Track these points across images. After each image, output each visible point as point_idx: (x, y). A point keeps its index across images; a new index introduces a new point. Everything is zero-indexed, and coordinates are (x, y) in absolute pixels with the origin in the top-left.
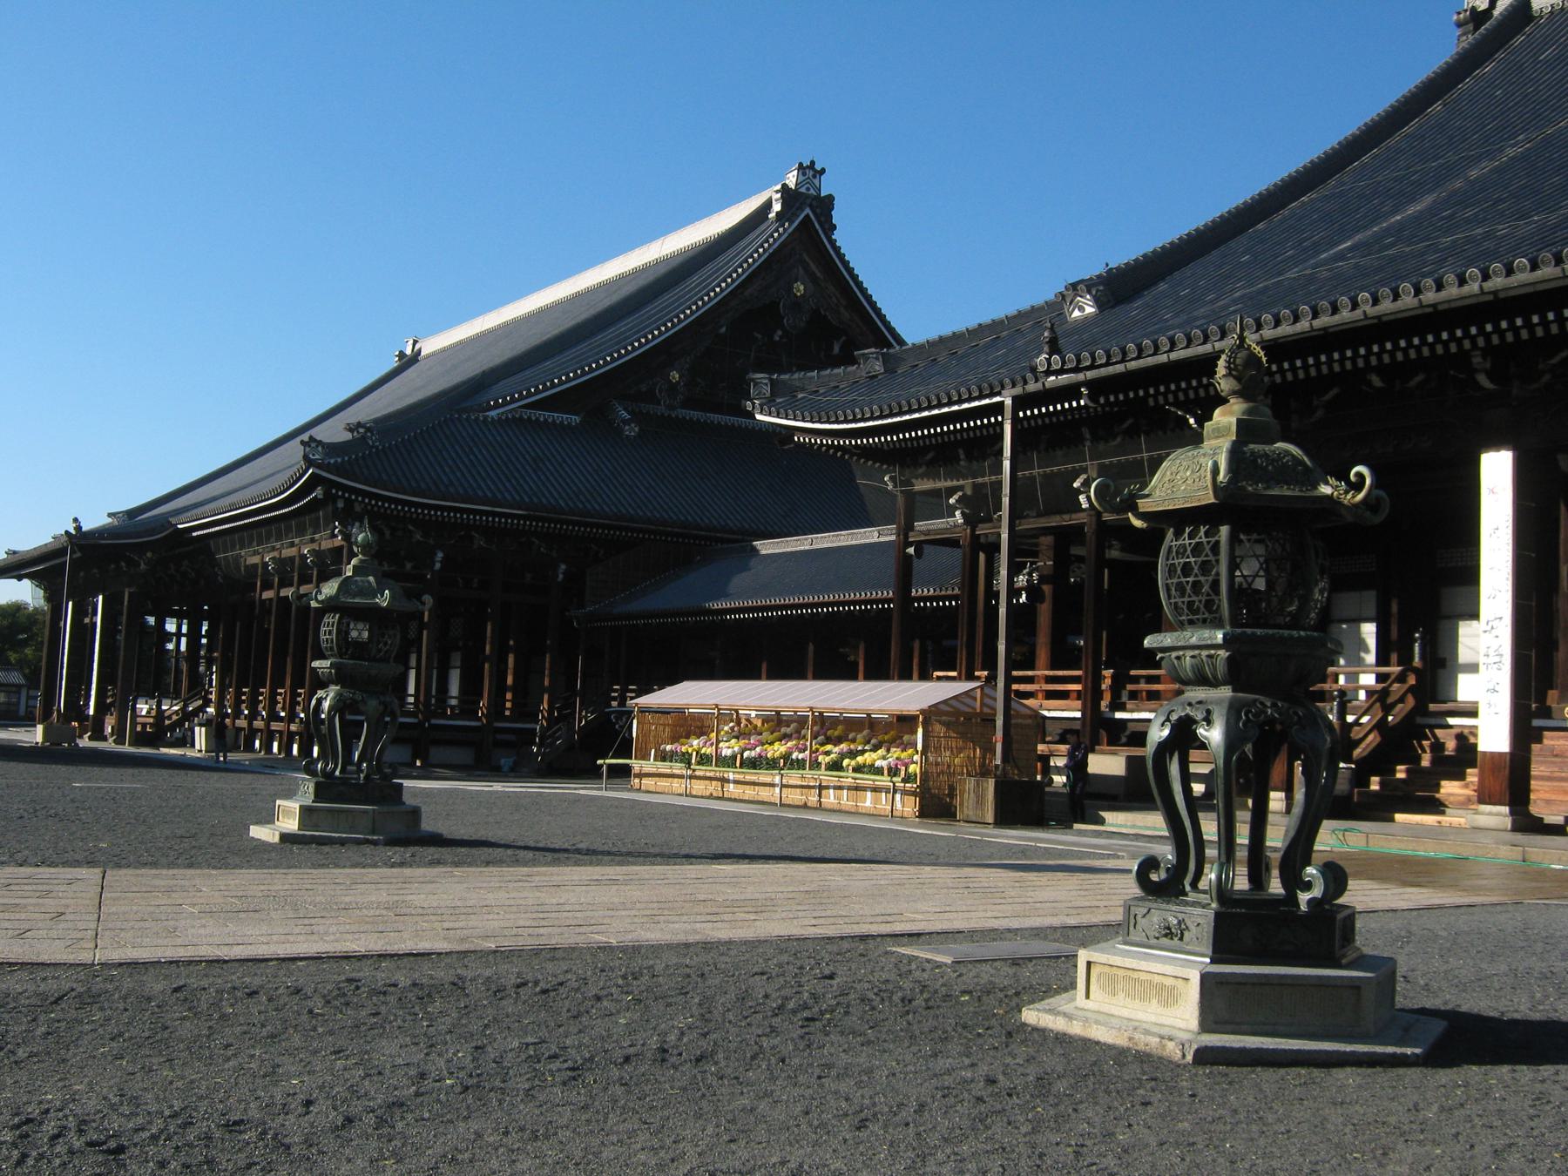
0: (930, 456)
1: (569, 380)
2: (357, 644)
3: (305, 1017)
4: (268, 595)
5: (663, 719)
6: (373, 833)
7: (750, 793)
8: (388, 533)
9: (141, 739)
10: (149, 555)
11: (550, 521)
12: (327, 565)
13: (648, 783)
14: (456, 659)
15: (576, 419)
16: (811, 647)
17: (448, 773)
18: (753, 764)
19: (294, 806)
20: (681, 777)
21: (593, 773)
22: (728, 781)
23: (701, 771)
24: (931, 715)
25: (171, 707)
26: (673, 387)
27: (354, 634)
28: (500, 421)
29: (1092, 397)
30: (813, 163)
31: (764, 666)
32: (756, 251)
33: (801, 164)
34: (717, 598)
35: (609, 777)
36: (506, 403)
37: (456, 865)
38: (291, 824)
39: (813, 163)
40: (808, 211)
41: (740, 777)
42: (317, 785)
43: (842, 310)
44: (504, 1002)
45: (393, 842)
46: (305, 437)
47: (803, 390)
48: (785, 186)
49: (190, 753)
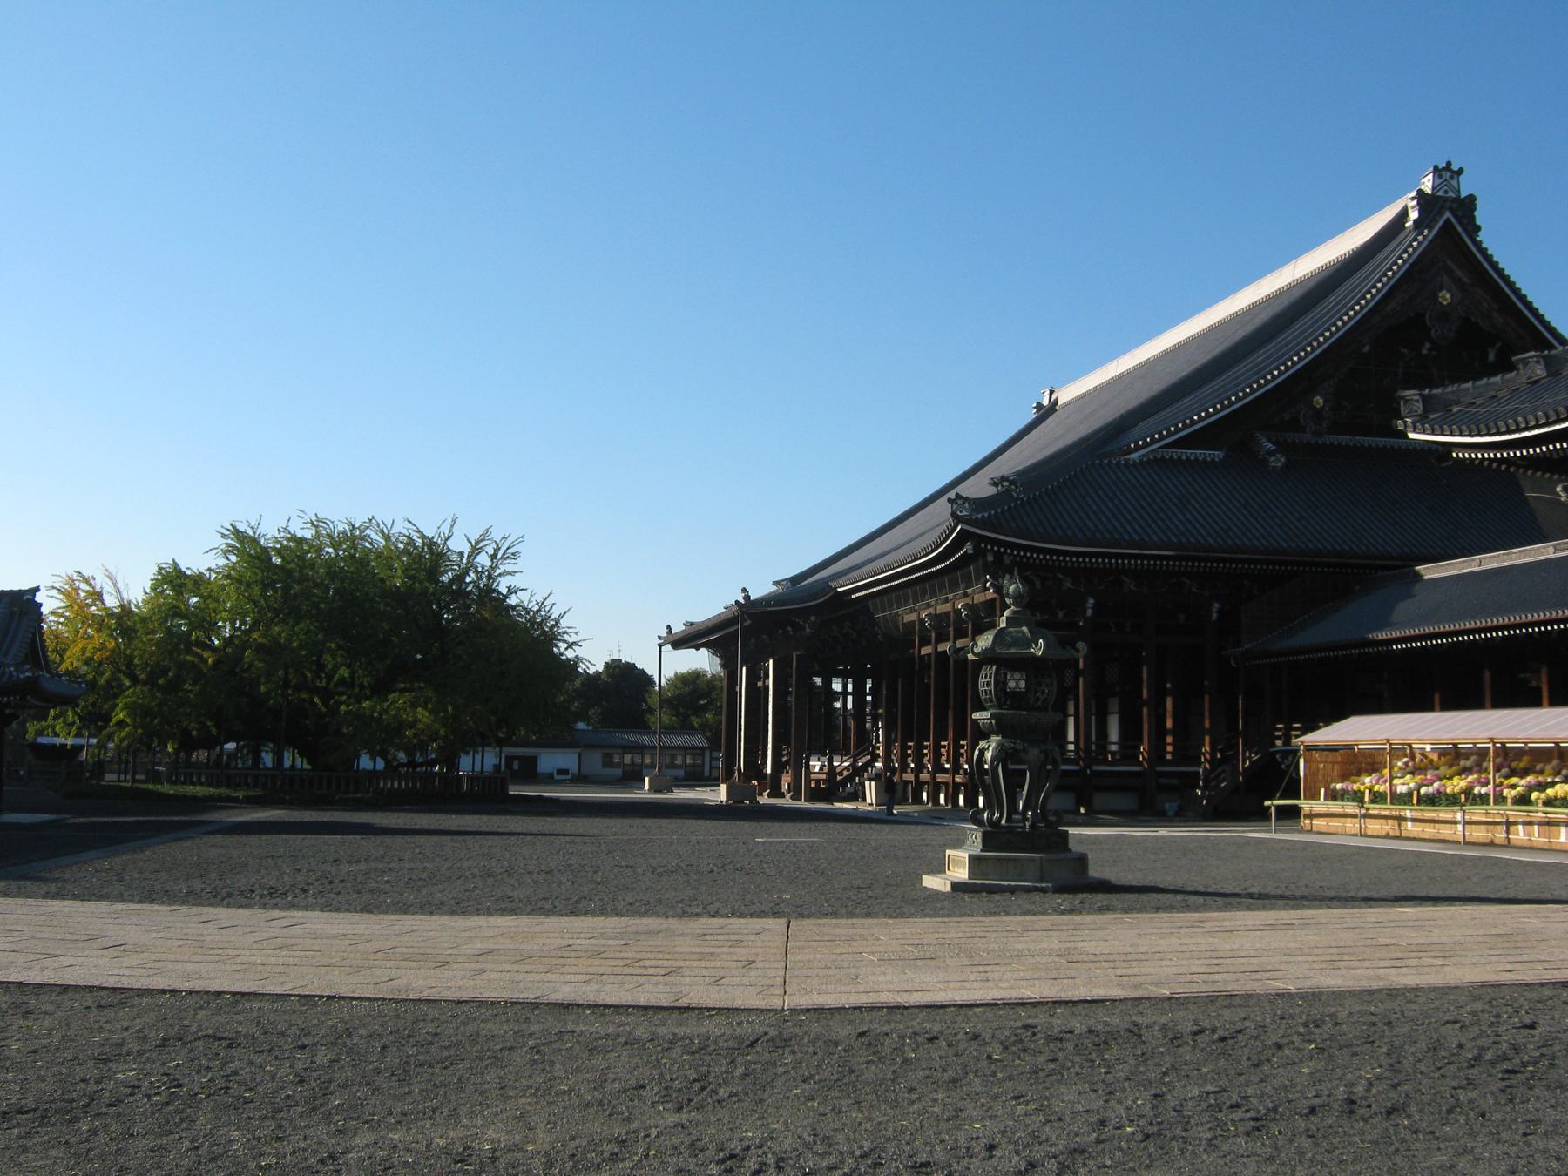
1: (1208, 415)
2: (1015, 694)
3: (984, 1063)
4: (926, 650)
5: (1331, 757)
6: (1042, 881)
7: (1430, 831)
8: (1038, 585)
9: (815, 795)
10: (813, 618)
11: (1200, 559)
12: (981, 619)
13: (1319, 823)
14: (1114, 704)
15: (1218, 455)
16: (1487, 675)
17: (1115, 819)
18: (1431, 800)
19: (963, 855)
20: (1354, 816)
21: (1261, 816)
22: (1405, 819)
23: (1375, 809)
25: (842, 763)
26: (1318, 413)
27: (1012, 684)
28: (1141, 464)
30: (1449, 164)
31: (1437, 698)
32: (1395, 263)
33: (1436, 170)
34: (1380, 628)
35: (1278, 818)
36: (1146, 445)
37: (1126, 911)
38: (961, 874)
39: (1449, 164)
40: (1449, 216)
41: (1418, 815)
42: (985, 835)
43: (1495, 315)
44: (1182, 1050)
45: (1061, 889)
46: (952, 495)
47: (1458, 403)
48: (1420, 192)
49: (862, 807)
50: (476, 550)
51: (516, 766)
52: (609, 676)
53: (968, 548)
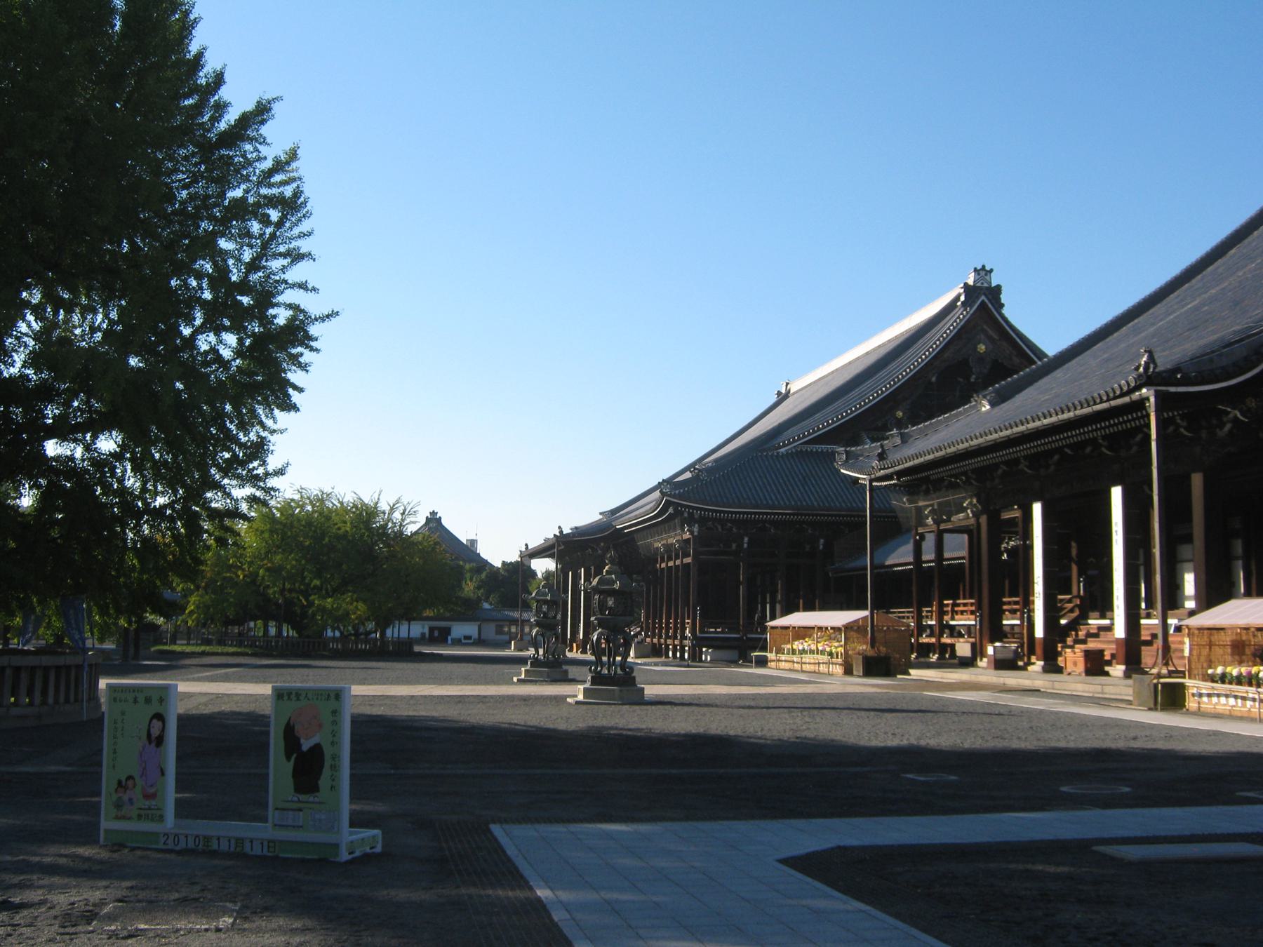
0: (924, 487)
4: (663, 565)
21: (747, 660)
24: (848, 627)
28: (789, 455)
29: (898, 479)
33: (975, 270)
40: (983, 299)
48: (966, 284)
50: (392, 509)
51: (436, 633)
52: (506, 570)
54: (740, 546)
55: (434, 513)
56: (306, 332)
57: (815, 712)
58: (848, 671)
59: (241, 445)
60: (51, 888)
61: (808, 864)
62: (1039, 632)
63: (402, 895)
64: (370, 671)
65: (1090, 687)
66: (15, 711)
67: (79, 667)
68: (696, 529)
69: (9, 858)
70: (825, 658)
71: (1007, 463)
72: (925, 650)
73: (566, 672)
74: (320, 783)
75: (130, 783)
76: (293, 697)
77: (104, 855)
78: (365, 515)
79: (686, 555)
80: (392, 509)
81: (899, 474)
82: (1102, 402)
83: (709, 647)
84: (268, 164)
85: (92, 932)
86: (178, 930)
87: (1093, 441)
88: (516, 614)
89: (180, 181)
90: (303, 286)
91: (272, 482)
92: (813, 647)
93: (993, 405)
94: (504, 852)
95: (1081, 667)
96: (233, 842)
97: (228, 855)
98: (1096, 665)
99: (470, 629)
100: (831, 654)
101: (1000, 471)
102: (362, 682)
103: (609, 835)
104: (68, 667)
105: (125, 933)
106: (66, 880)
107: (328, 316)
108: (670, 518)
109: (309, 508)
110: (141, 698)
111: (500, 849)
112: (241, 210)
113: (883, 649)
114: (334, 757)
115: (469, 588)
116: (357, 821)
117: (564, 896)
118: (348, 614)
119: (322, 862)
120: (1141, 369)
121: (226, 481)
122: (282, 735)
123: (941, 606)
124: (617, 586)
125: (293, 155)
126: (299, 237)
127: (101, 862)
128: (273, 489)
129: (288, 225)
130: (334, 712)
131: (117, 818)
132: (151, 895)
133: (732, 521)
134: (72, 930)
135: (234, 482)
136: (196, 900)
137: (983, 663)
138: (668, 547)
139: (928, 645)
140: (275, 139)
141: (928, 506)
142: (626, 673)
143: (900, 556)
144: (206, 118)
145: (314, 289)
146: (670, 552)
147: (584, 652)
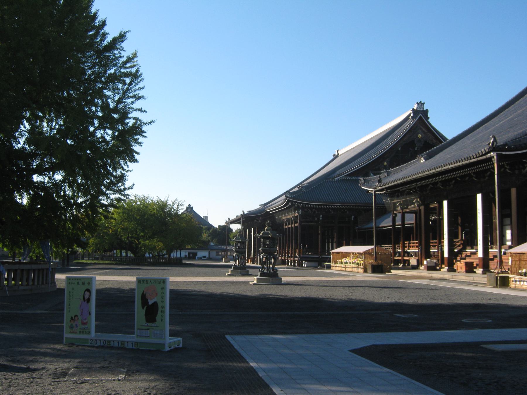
4: (286, 227)
21: (323, 267)
24: (365, 253)
28: (338, 180)
29: (386, 191)
33: (417, 103)
40: (420, 115)
50: (174, 203)
51: (191, 255)
52: (220, 229)
53: (290, 204)
54: (319, 218)
55: (190, 205)
56: (141, 129)
57: (354, 288)
58: (365, 271)
59: (114, 177)
60: (46, 362)
61: (362, 352)
62: (446, 255)
63: (194, 365)
64: (165, 271)
65: (469, 277)
66: (21, 288)
67: (47, 269)
68: (300, 212)
69: (26, 349)
70: (356, 265)
71: (432, 184)
72: (397, 262)
73: (248, 271)
74: (157, 318)
75: (76, 318)
76: (145, 282)
77: (66, 348)
78: (162, 206)
79: (296, 222)
80: (174, 203)
81: (387, 189)
82: (474, 158)
83: (306, 261)
84: (124, 59)
85: (66, 381)
86: (102, 380)
87: (469, 175)
88: (224, 247)
89: (88, 66)
90: (140, 110)
91: (127, 192)
92: (350, 261)
93: (426, 159)
94: (233, 347)
95: (464, 269)
96: (120, 343)
97: (119, 348)
98: (470, 268)
99: (205, 253)
100: (358, 264)
101: (429, 188)
102: (173, 275)
103: (275, 340)
104: (43, 269)
105: (80, 381)
106: (52, 359)
107: (150, 123)
108: (290, 207)
109: (139, 203)
110: (81, 283)
111: (231, 346)
112: (114, 78)
113: (380, 262)
114: (162, 307)
115: (205, 236)
116: (173, 334)
117: (262, 365)
118: (155, 247)
119: (157, 351)
120: (491, 145)
121: (108, 192)
122: (140, 298)
123: (404, 244)
124: (270, 235)
125: (135, 55)
126: (139, 89)
127: (65, 351)
128: (128, 195)
129: (134, 84)
130: (163, 288)
131: (71, 333)
132: (88, 365)
133: (315, 208)
134: (58, 380)
135: (111, 192)
136: (108, 367)
137: (422, 268)
138: (289, 219)
139: (398, 260)
140: (127, 48)
141: (398, 202)
142: (274, 272)
143: (386, 223)
144: (98, 40)
145: (145, 111)
146: (289, 221)
147: (253, 263)
